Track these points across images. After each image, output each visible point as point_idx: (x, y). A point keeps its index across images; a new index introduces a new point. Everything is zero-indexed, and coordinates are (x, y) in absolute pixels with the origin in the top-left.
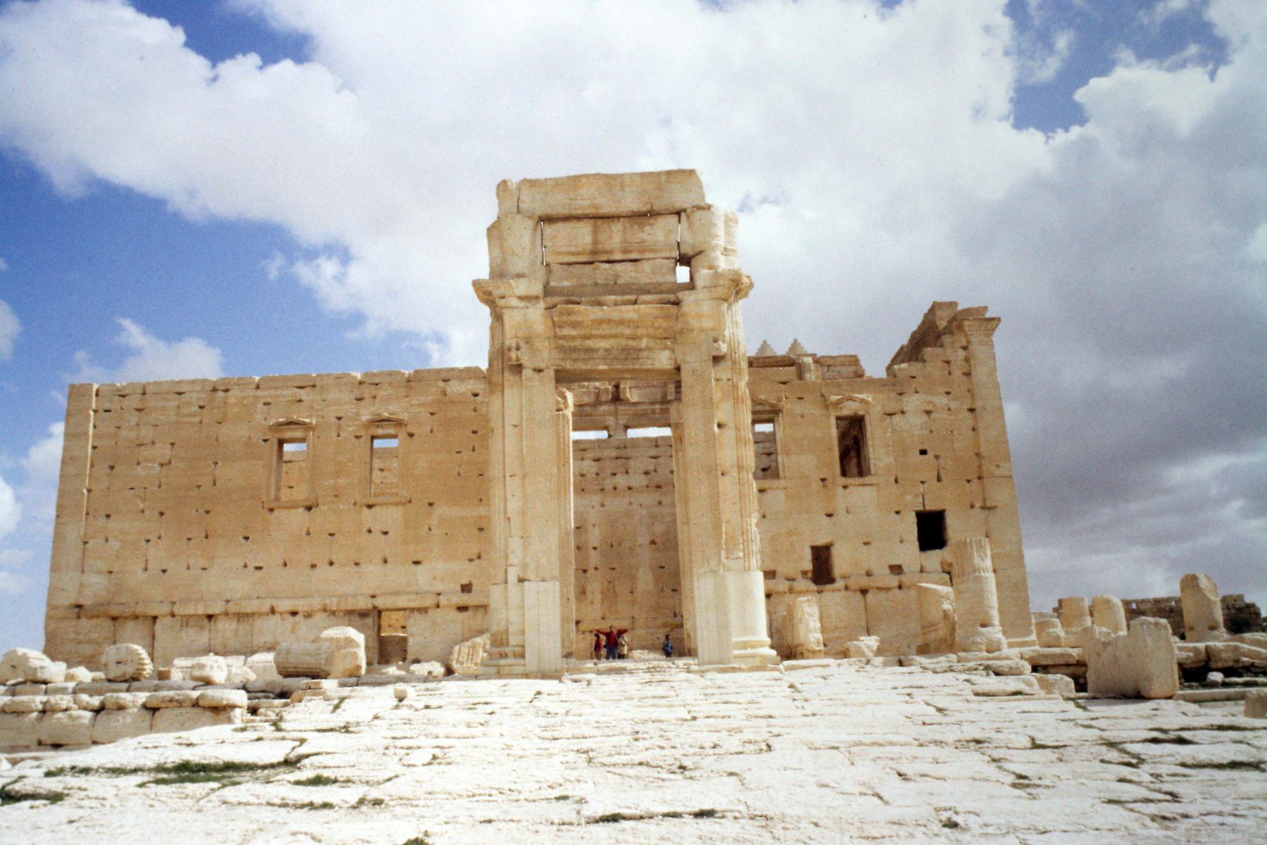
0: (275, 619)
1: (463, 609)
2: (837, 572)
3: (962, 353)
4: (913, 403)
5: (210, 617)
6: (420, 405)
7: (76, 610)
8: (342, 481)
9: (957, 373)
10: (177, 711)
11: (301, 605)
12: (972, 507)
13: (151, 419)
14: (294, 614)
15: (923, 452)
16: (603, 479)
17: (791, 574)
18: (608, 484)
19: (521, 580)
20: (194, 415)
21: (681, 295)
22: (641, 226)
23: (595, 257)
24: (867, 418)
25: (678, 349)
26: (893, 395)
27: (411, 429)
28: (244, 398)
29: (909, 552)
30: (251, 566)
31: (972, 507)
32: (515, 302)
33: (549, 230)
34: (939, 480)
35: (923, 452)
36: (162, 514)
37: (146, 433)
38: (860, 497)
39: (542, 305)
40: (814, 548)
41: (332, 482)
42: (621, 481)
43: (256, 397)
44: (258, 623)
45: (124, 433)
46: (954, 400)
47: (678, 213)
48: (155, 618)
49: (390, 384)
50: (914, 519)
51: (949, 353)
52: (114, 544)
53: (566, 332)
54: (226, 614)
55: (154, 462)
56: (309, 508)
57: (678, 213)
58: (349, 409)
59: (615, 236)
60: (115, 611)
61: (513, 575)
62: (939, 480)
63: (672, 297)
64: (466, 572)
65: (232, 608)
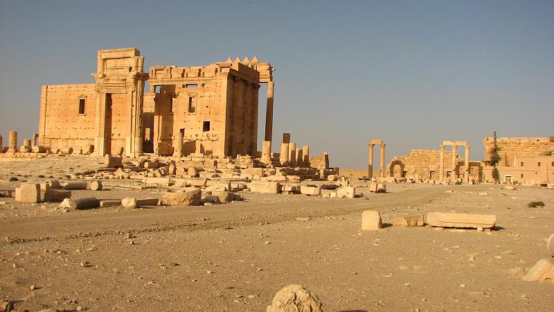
4: (207, 94)
37: (56, 98)
38: (192, 117)
50: (203, 123)
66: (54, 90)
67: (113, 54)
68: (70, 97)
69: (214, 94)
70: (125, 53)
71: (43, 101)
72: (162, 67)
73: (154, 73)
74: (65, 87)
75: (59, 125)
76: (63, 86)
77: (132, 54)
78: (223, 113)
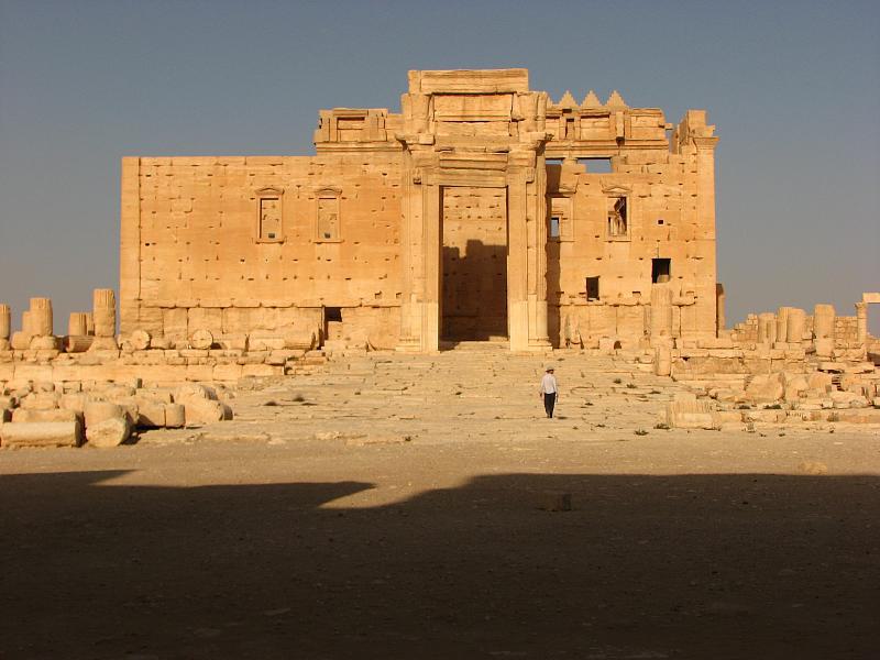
0: (262, 310)
1: (374, 307)
2: (601, 293)
3: (693, 158)
4: (658, 190)
5: (222, 308)
6: (350, 180)
7: (138, 303)
8: (302, 227)
9: (688, 172)
10: (253, 366)
11: (275, 303)
12: (688, 257)
13: (178, 182)
14: (274, 308)
15: (661, 222)
16: (461, 211)
17: (572, 293)
18: (464, 215)
19: (418, 301)
20: (205, 181)
21: (511, 145)
22: (491, 101)
23: (465, 119)
24: (628, 199)
25: (509, 176)
26: (647, 185)
27: (343, 195)
28: (237, 171)
29: (645, 282)
30: (246, 278)
31: (688, 257)
32: (419, 147)
33: (438, 100)
34: (669, 239)
35: (661, 222)
36: (188, 243)
37: (175, 192)
38: (621, 249)
39: (433, 148)
40: (588, 279)
41: (295, 228)
42: (474, 212)
43: (245, 171)
44: (254, 313)
45: (162, 192)
46: (683, 189)
47: (512, 93)
48: (188, 308)
49: (331, 166)
51: (684, 159)
52: (160, 262)
53: (446, 164)
54: (232, 307)
55: (180, 210)
56: (282, 243)
57: (512, 93)
58: (304, 180)
59: (476, 105)
60: (164, 304)
61: (414, 297)
62: (669, 239)
63: (505, 148)
64: (380, 286)
65: (235, 303)
66: (165, 170)
67: (459, 81)
68: (225, 191)
69: (675, 189)
70: (499, 81)
71: (129, 201)
72: (360, 111)
73: (333, 126)
74: (206, 163)
75: (188, 269)
76: (198, 160)
77: (521, 84)
78: (706, 237)
